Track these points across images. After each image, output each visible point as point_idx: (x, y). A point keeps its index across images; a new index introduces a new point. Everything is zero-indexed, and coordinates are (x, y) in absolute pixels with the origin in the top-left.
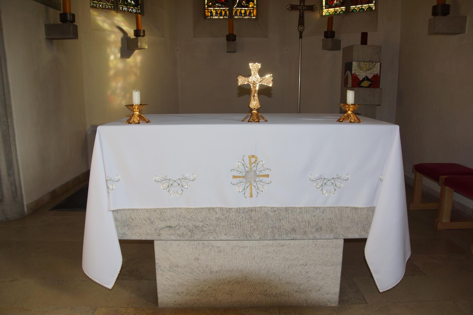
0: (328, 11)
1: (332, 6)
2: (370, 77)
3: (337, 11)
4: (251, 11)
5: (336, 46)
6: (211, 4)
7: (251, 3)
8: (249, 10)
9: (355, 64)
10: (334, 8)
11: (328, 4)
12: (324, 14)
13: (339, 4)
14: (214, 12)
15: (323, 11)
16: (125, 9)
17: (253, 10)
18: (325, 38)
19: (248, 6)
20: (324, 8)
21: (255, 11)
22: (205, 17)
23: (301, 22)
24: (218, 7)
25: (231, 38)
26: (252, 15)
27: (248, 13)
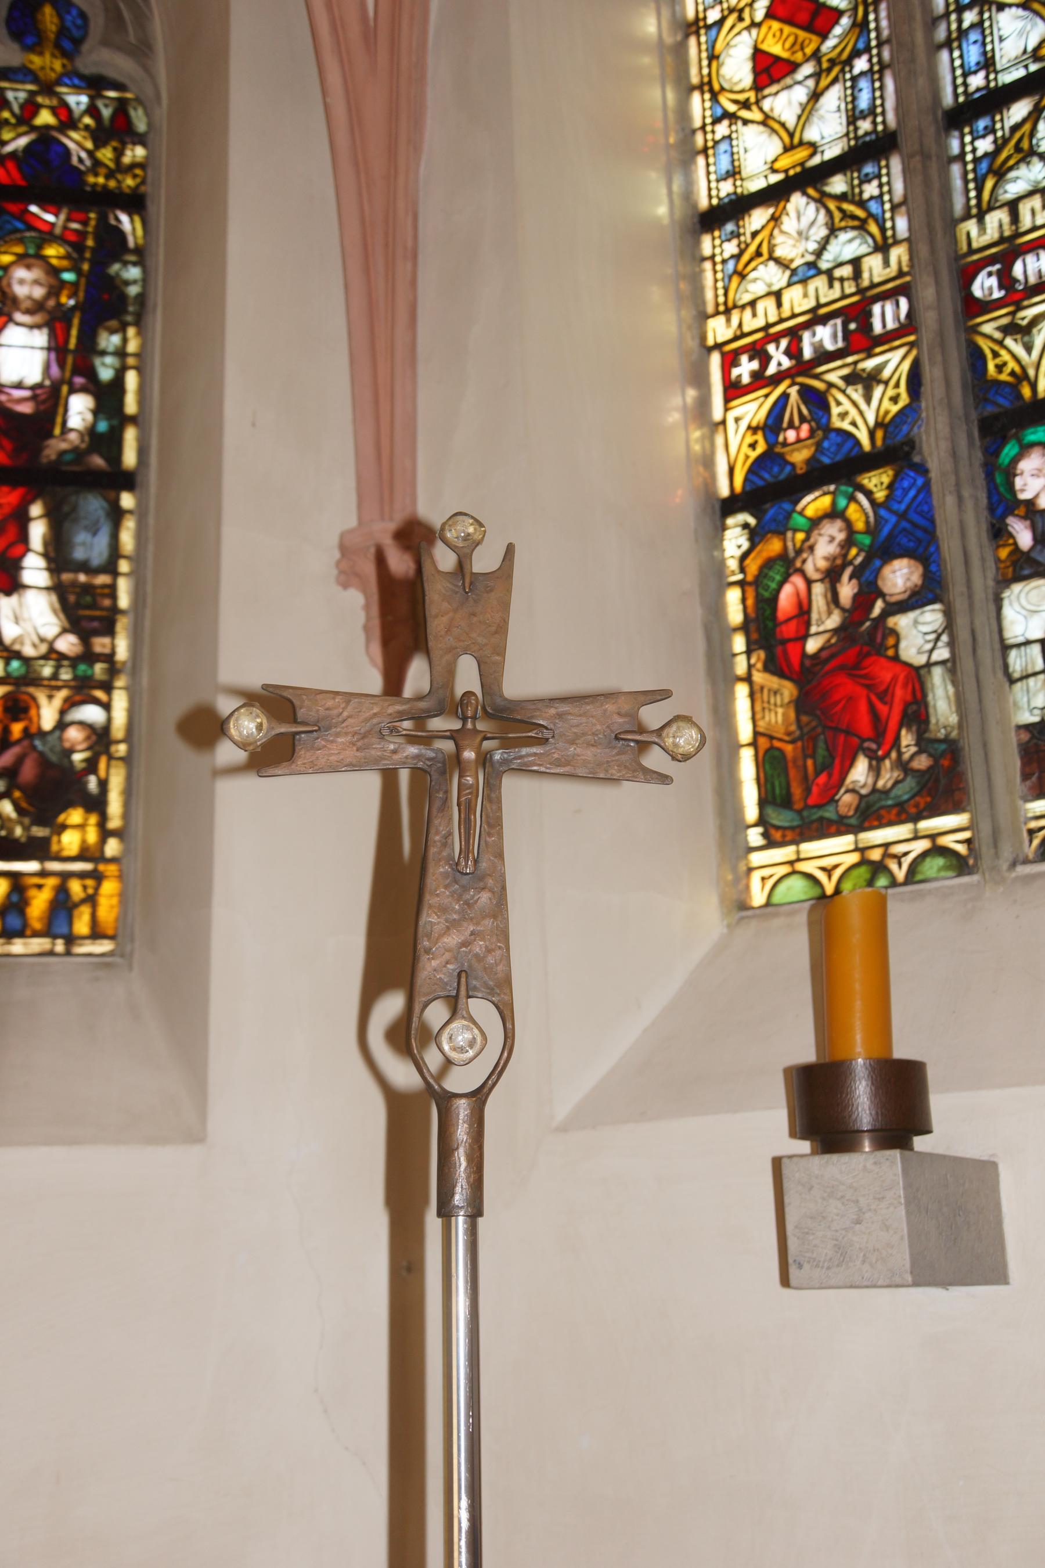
0: (791, 863)
1: (829, 813)
3: (886, 855)
4: (76, 888)
7: (75, 816)
8: (51, 882)
10: (856, 829)
11: (786, 803)
12: (758, 897)
13: (904, 791)
15: (750, 870)
17: (90, 882)
18: (804, 1146)
19: (46, 842)
26: (82, 925)
27: (39, 902)
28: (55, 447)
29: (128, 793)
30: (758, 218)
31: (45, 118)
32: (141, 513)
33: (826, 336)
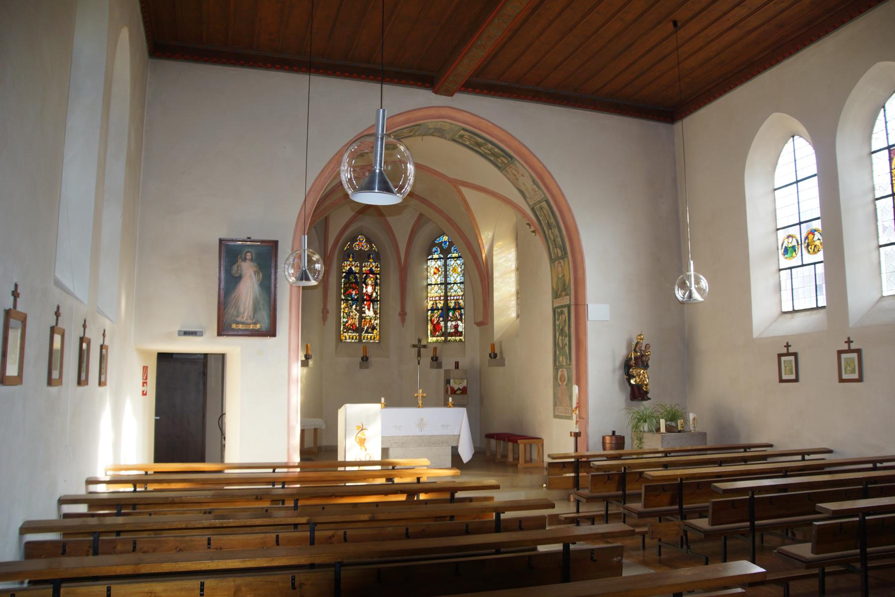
2: (461, 388)
5: (439, 366)
6: (345, 330)
7: (375, 330)
9: (452, 380)
12: (429, 342)
14: (347, 337)
20: (429, 337)
21: (378, 337)
22: (341, 340)
23: (419, 355)
24: (351, 333)
25: (365, 359)
27: (373, 338)
28: (372, 298)
29: (379, 328)
30: (433, 286)
31: (371, 266)
33: (437, 298)
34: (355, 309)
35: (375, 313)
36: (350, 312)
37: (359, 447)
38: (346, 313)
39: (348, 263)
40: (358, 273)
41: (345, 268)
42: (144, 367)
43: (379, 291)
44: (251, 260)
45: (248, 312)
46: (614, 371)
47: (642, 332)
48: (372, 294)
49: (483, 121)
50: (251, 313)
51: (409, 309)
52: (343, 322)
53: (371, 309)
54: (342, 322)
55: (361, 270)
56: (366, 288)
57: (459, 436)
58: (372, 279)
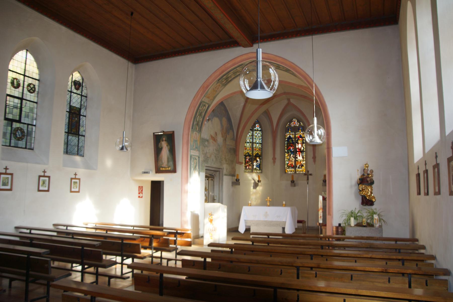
16: (256, 171)
21: (305, 170)
22: (286, 173)
24: (291, 169)
25: (293, 182)
26: (304, 171)
27: (302, 171)
31: (300, 134)
32: (305, 153)
34: (293, 157)
35: (303, 158)
36: (290, 158)
37: (210, 223)
38: (288, 159)
39: (289, 133)
40: (293, 138)
41: (287, 136)
42: (139, 187)
43: (305, 147)
44: (165, 140)
45: (166, 163)
46: (351, 187)
47: (367, 162)
48: (301, 148)
49: (269, 55)
50: (167, 163)
51: (317, 155)
52: (287, 163)
53: (301, 156)
54: (286, 163)
55: (295, 136)
56: (298, 145)
57: (286, 222)
58: (301, 140)
